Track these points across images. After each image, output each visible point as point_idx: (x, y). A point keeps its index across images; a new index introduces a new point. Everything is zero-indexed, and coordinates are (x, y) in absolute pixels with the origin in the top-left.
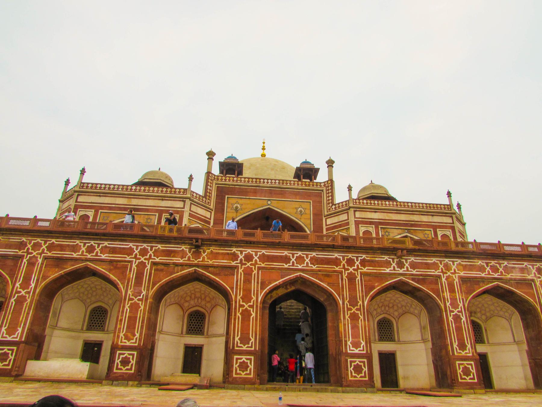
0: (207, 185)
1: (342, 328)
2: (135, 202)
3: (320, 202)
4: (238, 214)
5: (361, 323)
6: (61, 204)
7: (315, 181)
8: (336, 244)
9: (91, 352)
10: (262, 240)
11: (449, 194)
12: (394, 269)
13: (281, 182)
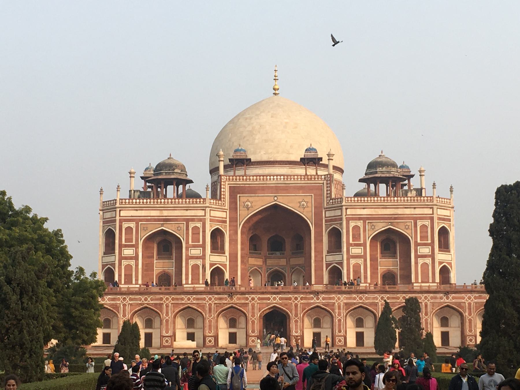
1: (291, 326)
3: (322, 195)
4: (250, 211)
5: (299, 324)
6: (101, 212)
7: (321, 162)
8: (290, 291)
9: (191, 337)
10: (259, 291)
11: (434, 185)
12: (315, 301)
13: (286, 177)
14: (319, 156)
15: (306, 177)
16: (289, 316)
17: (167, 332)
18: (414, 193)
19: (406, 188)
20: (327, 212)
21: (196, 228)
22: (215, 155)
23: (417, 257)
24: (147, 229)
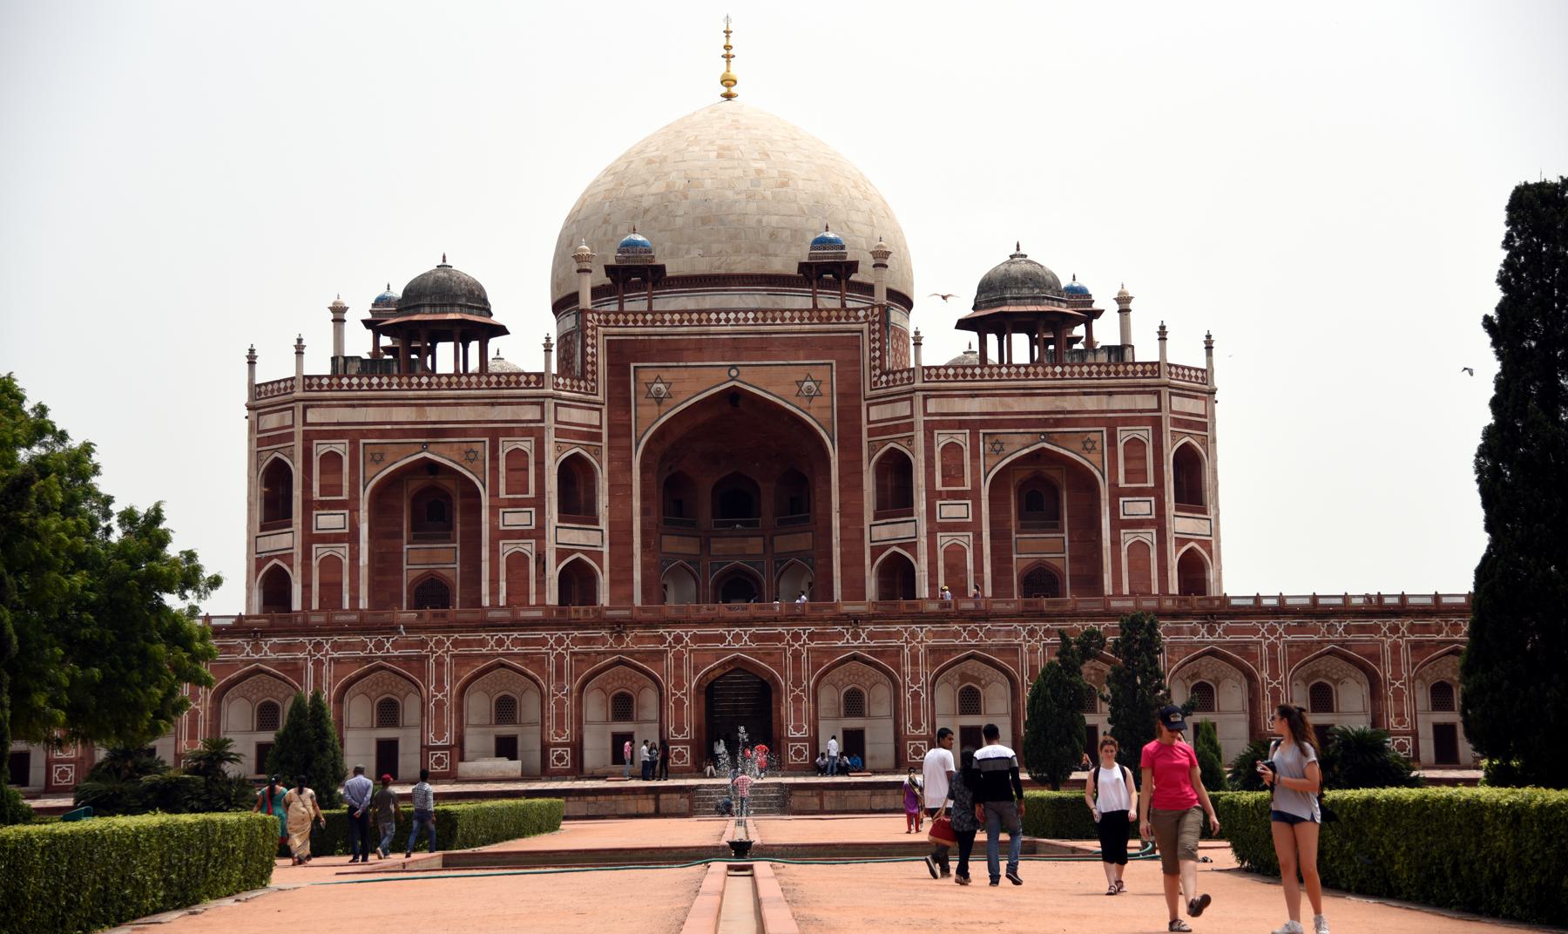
0: (584, 345)
1: (783, 712)
2: (433, 414)
3: (857, 362)
4: (664, 409)
6: (254, 414)
9: (506, 748)
11: (1162, 334)
12: (847, 641)
13: (760, 315)
14: (849, 258)
15: (815, 314)
16: (777, 683)
17: (439, 735)
18: (1103, 358)
19: (1079, 346)
20: (872, 409)
21: (517, 454)
22: (569, 259)
23: (1117, 525)
24: (382, 459)
